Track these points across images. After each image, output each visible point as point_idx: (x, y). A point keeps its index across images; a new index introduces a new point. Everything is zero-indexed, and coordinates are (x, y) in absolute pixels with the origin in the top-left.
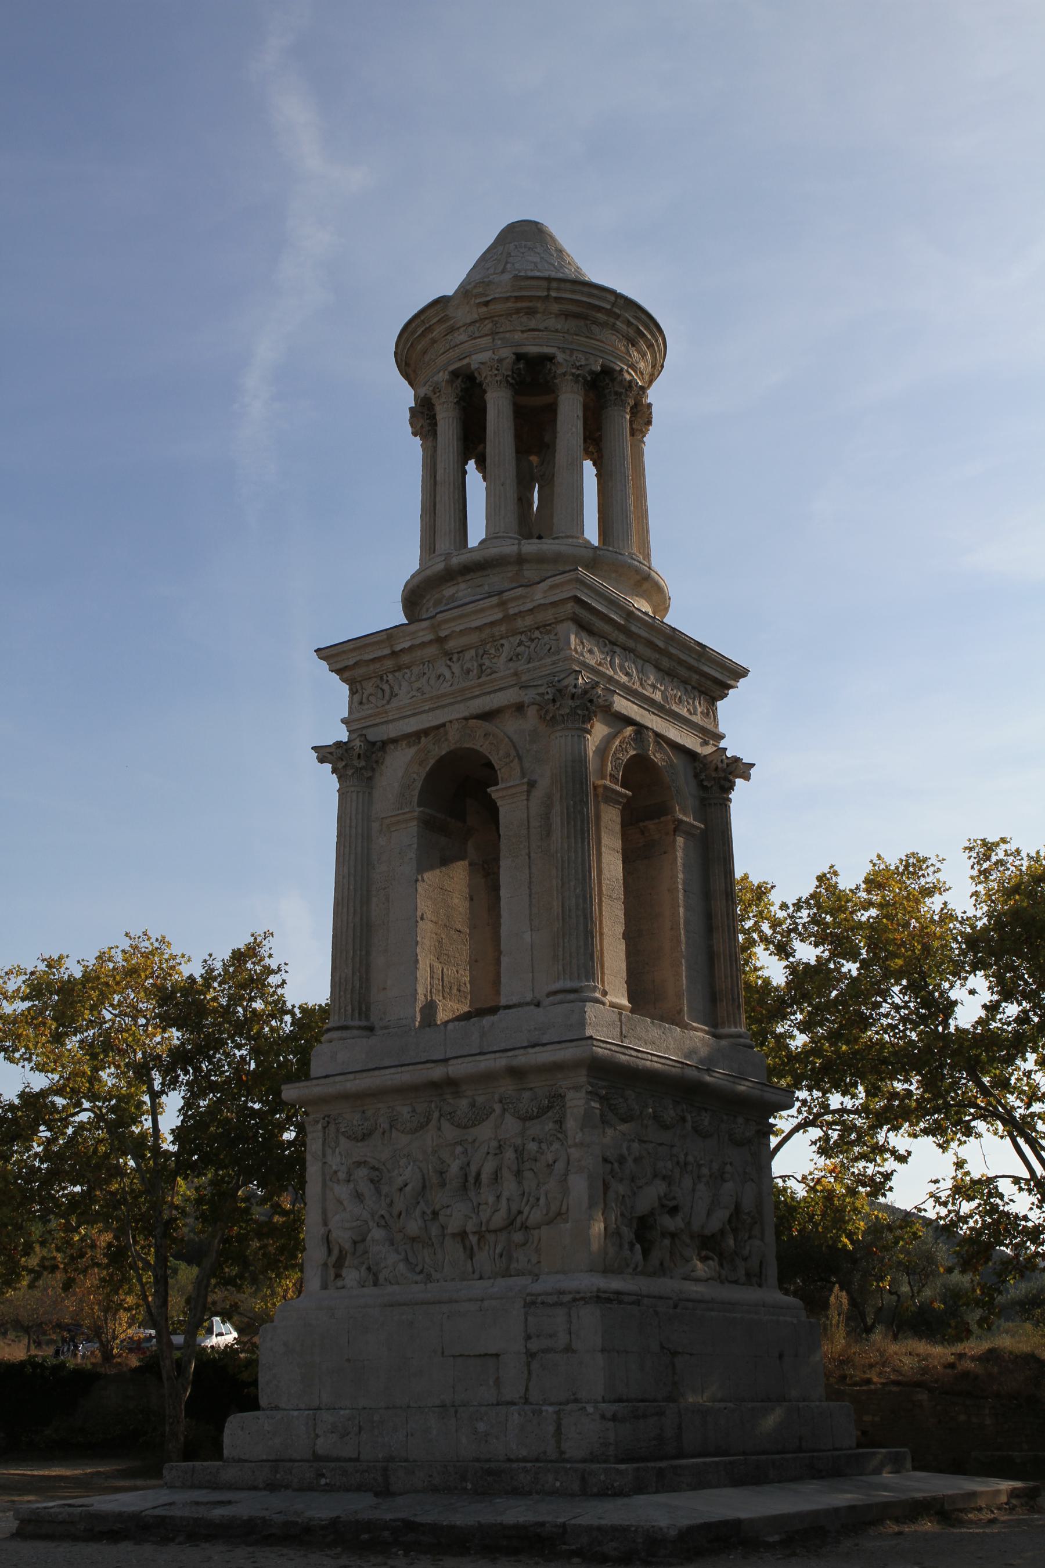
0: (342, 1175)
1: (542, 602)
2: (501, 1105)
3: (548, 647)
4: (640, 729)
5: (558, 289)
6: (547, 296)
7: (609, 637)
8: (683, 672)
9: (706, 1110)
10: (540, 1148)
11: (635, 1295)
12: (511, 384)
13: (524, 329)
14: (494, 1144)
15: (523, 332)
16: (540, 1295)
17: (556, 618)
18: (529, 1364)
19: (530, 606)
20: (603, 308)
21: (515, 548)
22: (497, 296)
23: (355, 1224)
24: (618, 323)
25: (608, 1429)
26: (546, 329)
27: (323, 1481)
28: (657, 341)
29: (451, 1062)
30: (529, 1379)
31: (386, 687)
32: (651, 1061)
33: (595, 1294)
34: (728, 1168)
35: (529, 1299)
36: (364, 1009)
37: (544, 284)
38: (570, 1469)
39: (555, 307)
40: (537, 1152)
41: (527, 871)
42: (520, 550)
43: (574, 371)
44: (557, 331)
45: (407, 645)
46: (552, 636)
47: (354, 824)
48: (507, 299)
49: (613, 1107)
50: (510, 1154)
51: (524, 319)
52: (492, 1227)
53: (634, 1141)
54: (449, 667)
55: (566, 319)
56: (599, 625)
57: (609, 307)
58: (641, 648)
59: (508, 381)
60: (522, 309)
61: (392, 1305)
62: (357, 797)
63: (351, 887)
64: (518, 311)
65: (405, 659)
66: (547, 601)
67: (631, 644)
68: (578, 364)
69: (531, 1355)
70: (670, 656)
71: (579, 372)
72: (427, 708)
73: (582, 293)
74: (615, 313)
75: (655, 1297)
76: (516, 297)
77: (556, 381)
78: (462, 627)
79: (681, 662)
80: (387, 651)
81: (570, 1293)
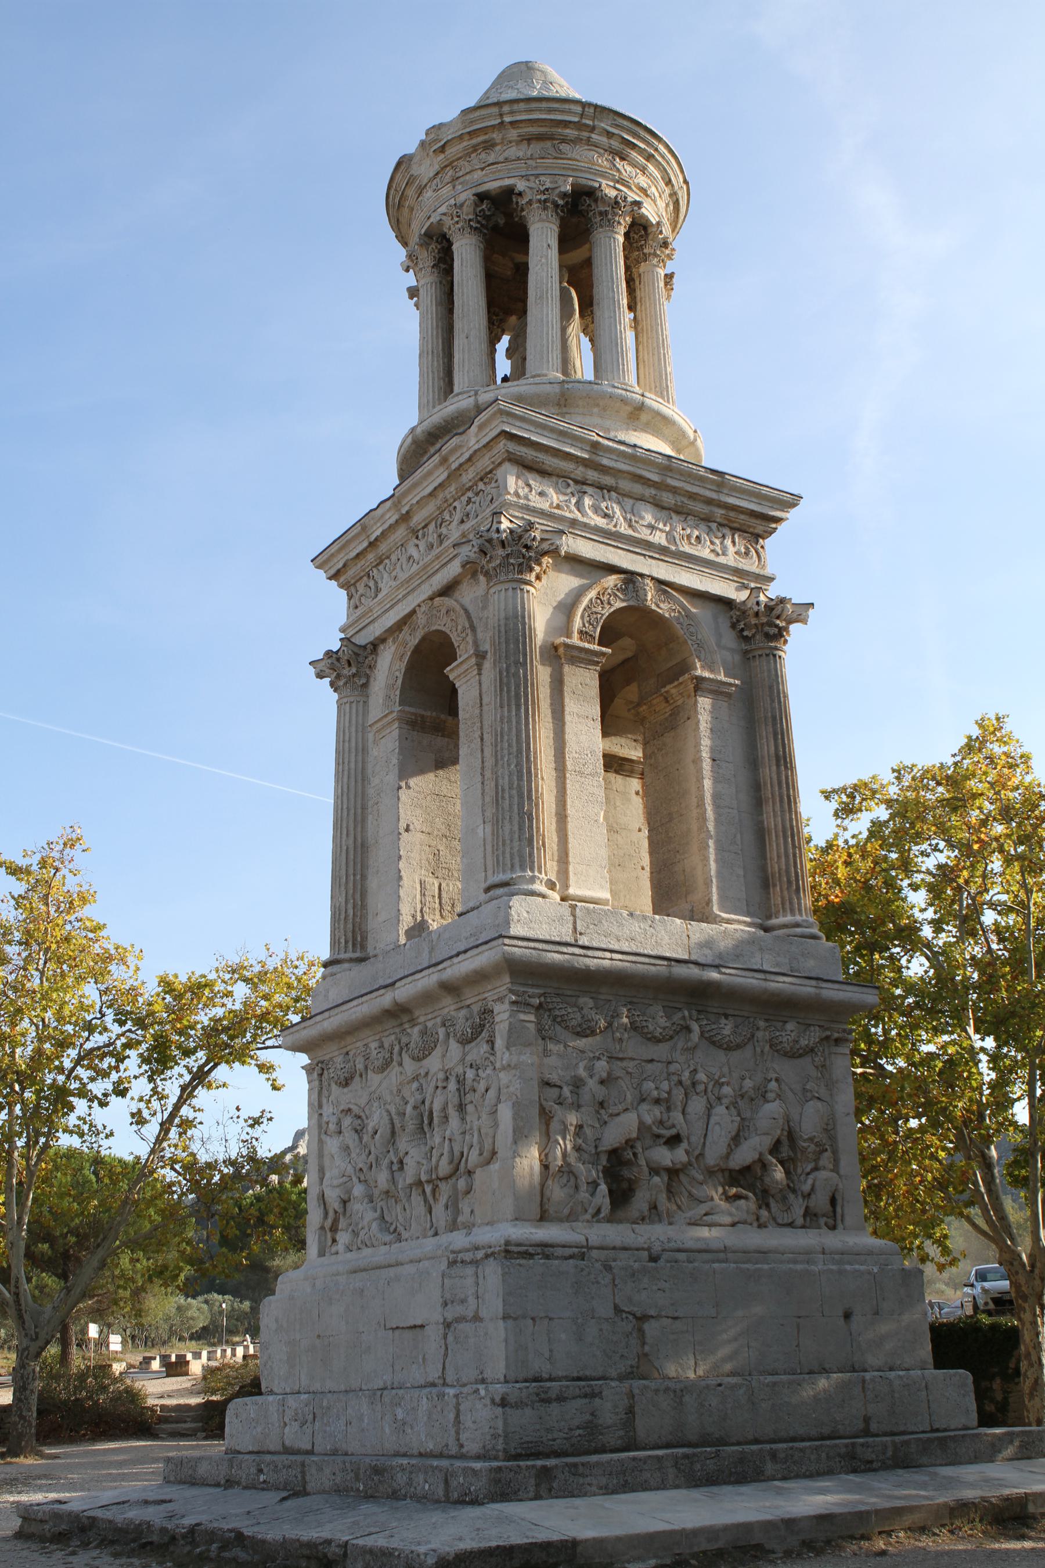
0: (332, 1127)
1: (476, 447)
2: (443, 1029)
3: (490, 497)
4: (631, 578)
5: (512, 113)
6: (502, 123)
7: (572, 476)
8: (699, 507)
9: (726, 1016)
10: (478, 1075)
11: (577, 1247)
12: (476, 229)
13: (483, 165)
14: (441, 1076)
15: (482, 169)
16: (460, 1252)
17: (493, 463)
18: (445, 1337)
19: (467, 456)
20: (570, 122)
21: (472, 400)
22: (450, 137)
23: (341, 1180)
24: (593, 136)
25: (497, 1417)
26: (506, 160)
27: (262, 1478)
28: (656, 150)
29: (398, 984)
30: (446, 1355)
31: (371, 584)
32: (611, 959)
33: (502, 1248)
34: (773, 1085)
35: (451, 1256)
36: (359, 939)
37: (495, 110)
38: (437, 1467)
39: (513, 134)
40: (474, 1080)
41: (479, 756)
42: (476, 401)
43: (538, 197)
44: (518, 159)
45: (378, 533)
46: (493, 485)
47: (347, 738)
48: (461, 137)
49: (559, 1019)
50: (452, 1086)
51: (483, 155)
52: (441, 1175)
53: (599, 1059)
54: (417, 546)
55: (529, 144)
56: (550, 462)
57: (576, 119)
58: (625, 485)
59: (471, 227)
60: (479, 144)
61: (355, 1272)
62: (350, 708)
63: (345, 807)
64: (475, 148)
65: (383, 548)
66: (481, 445)
67: (608, 480)
68: (542, 189)
69: (447, 1325)
70: (674, 490)
71: (543, 197)
72: (400, 596)
73: (540, 110)
74: (586, 125)
75: (614, 1248)
76: (469, 133)
77: (524, 213)
78: (418, 498)
79: (692, 496)
80: (365, 544)
81: (484, 1248)
